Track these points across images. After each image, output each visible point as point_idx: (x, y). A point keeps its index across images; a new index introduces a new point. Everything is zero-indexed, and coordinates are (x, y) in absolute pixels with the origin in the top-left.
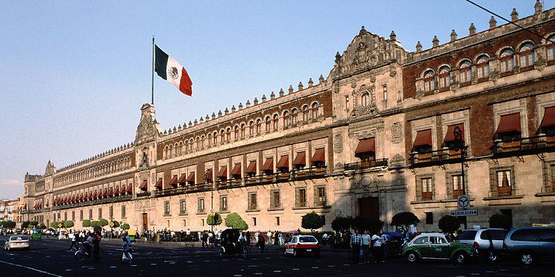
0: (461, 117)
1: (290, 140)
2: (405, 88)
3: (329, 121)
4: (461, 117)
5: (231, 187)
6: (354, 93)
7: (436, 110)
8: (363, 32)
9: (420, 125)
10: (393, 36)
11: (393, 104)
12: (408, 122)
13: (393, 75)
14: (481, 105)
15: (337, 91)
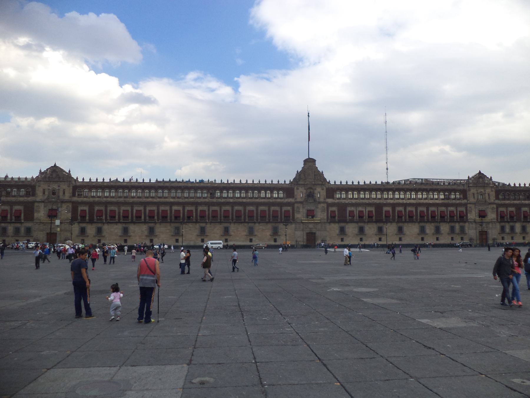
0: (512, 209)
1: (446, 205)
2: (496, 197)
3: (465, 201)
4: (512, 209)
5: (406, 222)
6: (477, 193)
7: (506, 206)
8: (480, 172)
9: (501, 209)
10: (491, 178)
11: (493, 201)
12: (497, 208)
13: (492, 191)
14: (518, 207)
15: (469, 190)
